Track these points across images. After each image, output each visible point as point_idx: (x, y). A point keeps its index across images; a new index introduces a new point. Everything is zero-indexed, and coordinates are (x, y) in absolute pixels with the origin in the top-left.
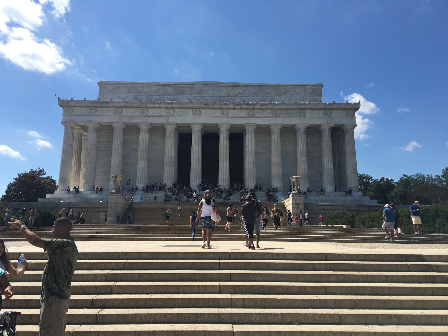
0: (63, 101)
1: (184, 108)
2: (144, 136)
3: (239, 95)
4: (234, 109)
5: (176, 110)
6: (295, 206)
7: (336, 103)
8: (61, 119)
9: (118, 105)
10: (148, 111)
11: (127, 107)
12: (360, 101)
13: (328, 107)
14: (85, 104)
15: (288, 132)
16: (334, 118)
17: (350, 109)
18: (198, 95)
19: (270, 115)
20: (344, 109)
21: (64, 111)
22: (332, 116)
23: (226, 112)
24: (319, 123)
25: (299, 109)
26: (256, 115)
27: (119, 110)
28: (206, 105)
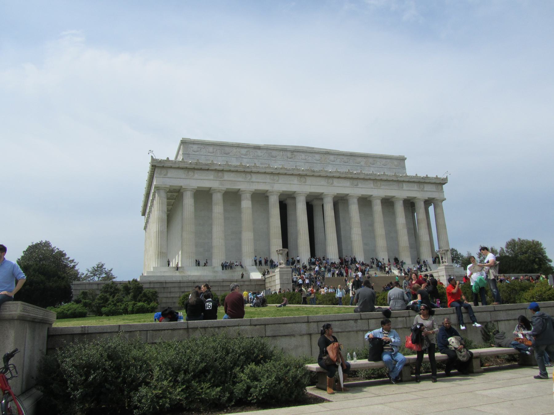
0: (156, 160)
1: (289, 175)
2: (246, 204)
3: (331, 163)
4: (339, 178)
5: (281, 176)
7: (428, 177)
9: (221, 168)
11: (230, 171)
13: (423, 181)
16: (427, 191)
18: (290, 160)
19: (372, 186)
22: (425, 189)
23: (330, 181)
26: (360, 185)
27: (220, 174)
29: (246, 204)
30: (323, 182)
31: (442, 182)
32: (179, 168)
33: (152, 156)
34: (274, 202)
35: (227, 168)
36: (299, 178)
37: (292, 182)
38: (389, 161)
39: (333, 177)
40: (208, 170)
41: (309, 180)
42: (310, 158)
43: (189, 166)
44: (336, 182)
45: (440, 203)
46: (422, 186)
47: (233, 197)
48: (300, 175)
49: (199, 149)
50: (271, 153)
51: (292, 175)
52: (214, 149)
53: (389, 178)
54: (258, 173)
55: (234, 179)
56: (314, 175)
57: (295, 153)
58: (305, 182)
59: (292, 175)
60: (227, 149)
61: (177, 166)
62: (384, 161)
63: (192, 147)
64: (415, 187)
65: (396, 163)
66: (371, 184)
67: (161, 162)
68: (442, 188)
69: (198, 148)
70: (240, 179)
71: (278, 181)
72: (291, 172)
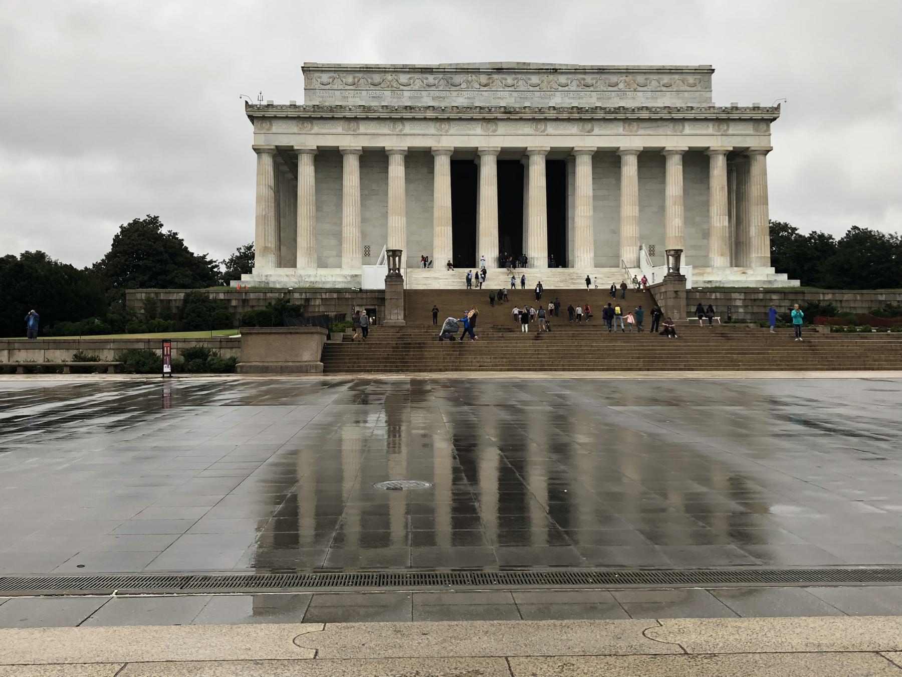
0: (252, 106)
2: (397, 170)
3: (560, 89)
4: (557, 119)
5: (452, 123)
6: (673, 295)
7: (737, 108)
10: (403, 124)
11: (367, 119)
12: (779, 105)
13: (724, 116)
15: (652, 161)
17: (763, 120)
18: (485, 89)
19: (620, 130)
20: (751, 120)
22: (731, 132)
23: (541, 126)
25: (672, 120)
26: (597, 131)
27: (353, 125)
28: (505, 113)
29: (397, 170)
30: (527, 128)
31: (766, 116)
32: (287, 118)
33: (246, 102)
35: (363, 115)
36: (484, 124)
38: (676, 77)
39: (546, 119)
40: (333, 118)
41: (502, 128)
42: (521, 83)
43: (302, 115)
44: (551, 128)
45: (760, 158)
46: (724, 127)
51: (472, 119)
52: (354, 78)
53: (653, 116)
54: (414, 119)
55: (375, 131)
56: (510, 115)
57: (495, 76)
59: (472, 119)
60: (377, 78)
61: (284, 114)
62: (666, 79)
63: (320, 77)
64: (710, 129)
65: (691, 79)
66: (620, 129)
67: (259, 108)
68: (768, 126)
70: (386, 130)
71: (447, 131)
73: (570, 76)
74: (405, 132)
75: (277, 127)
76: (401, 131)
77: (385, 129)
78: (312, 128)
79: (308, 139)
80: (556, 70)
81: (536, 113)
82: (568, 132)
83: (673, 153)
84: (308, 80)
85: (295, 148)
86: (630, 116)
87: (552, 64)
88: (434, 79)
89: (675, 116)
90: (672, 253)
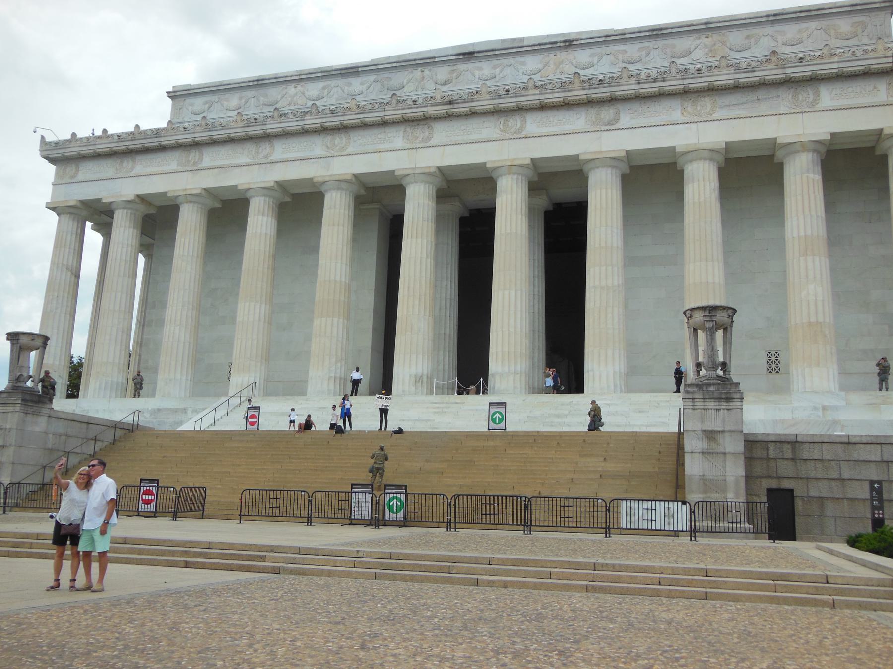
4: (543, 107)
8: (46, 193)
11: (213, 143)
14: (102, 147)
21: (57, 174)
23: (515, 122)
24: (874, 125)
25: (788, 82)
27: (194, 155)
29: (260, 224)
30: (488, 129)
33: (42, 137)
34: (337, 212)
37: (382, 147)
38: (813, 25)
41: (441, 132)
42: (508, 71)
44: (534, 124)
47: (226, 214)
48: (405, 121)
49: (207, 106)
50: (390, 79)
51: (384, 124)
52: (241, 98)
53: (744, 78)
55: (226, 162)
57: (462, 67)
58: (429, 138)
66: (673, 110)
69: (206, 102)
71: (343, 149)
72: (376, 116)
73: (598, 50)
74: (273, 158)
75: (88, 170)
76: (266, 157)
77: (242, 155)
78: (133, 169)
79: (123, 185)
80: (570, 41)
81: (500, 97)
82: (568, 128)
83: (791, 148)
84: (175, 110)
85: (104, 201)
86: (693, 83)
87: (563, 35)
88: (362, 84)
89: (793, 71)
90: (699, 317)
